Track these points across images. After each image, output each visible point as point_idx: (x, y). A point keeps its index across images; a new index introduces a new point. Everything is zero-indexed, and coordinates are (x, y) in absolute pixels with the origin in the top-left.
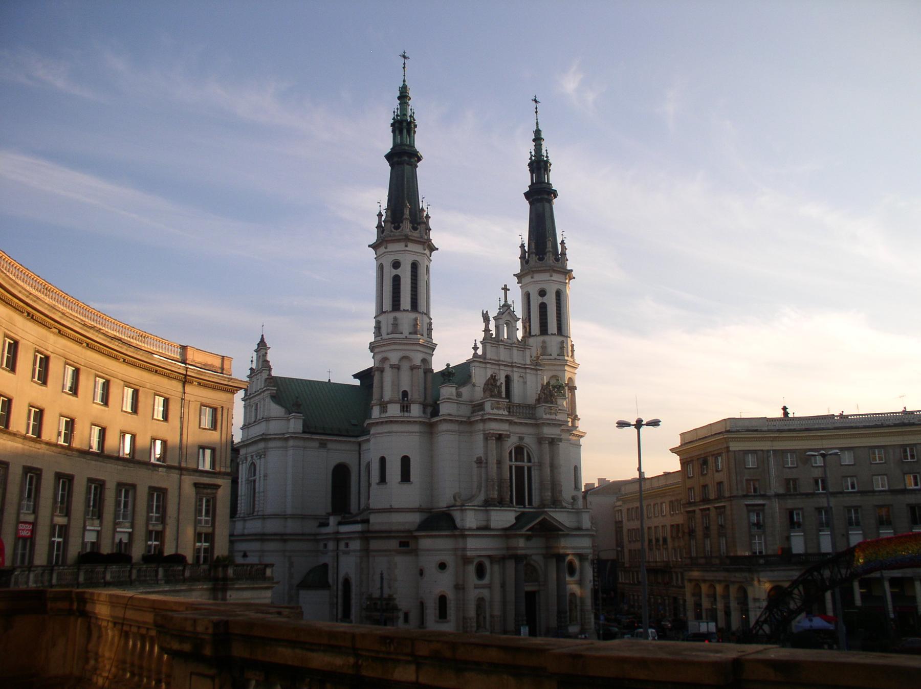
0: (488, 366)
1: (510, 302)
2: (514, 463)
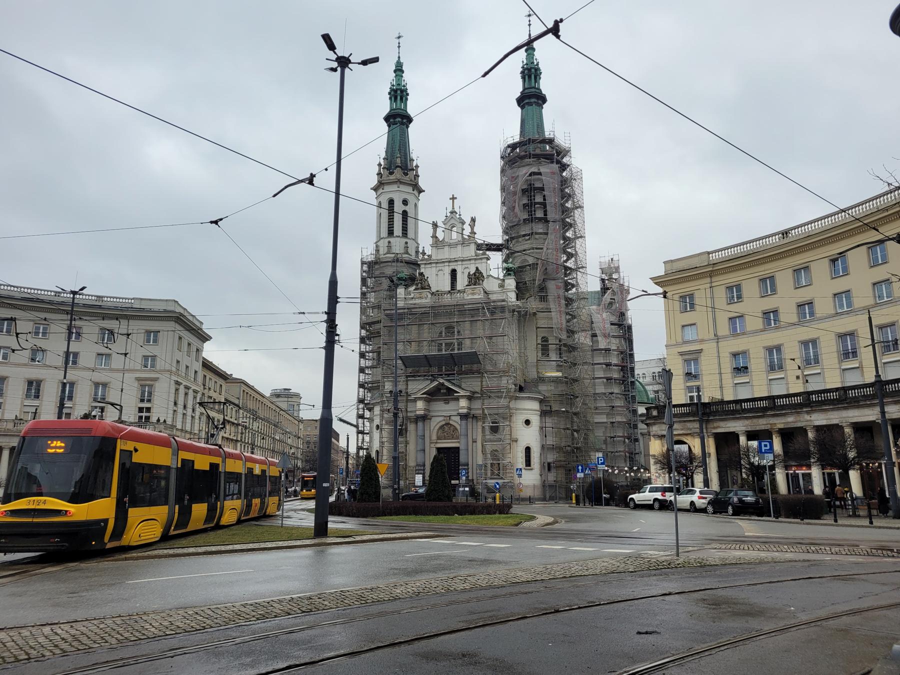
1: (457, 210)
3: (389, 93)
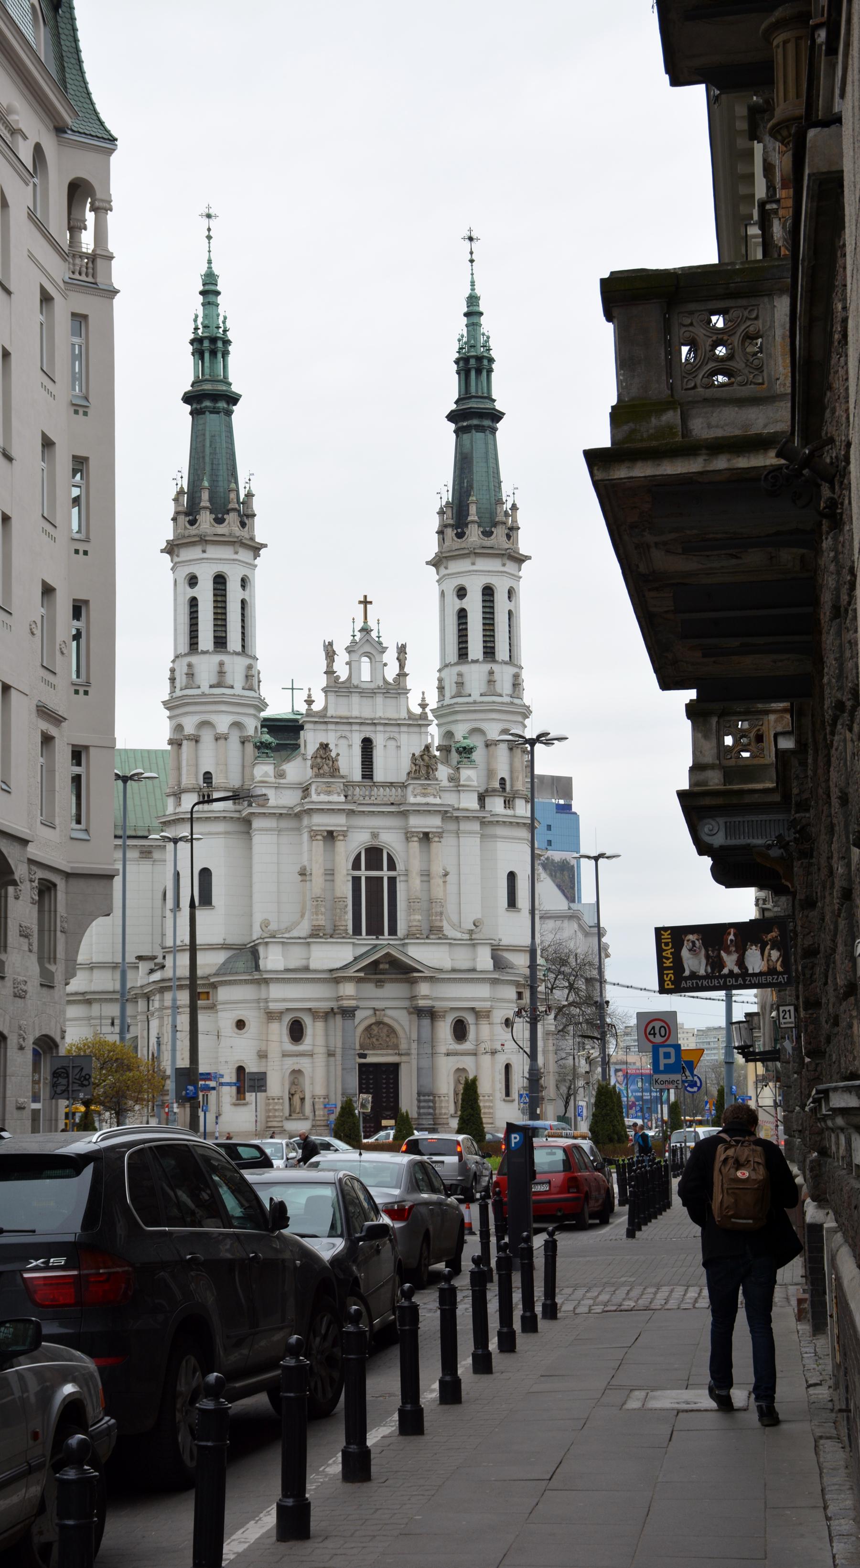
0: (331, 727)
1: (372, 623)
2: (363, 873)
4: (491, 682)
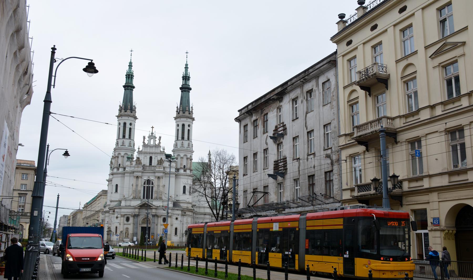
1: (153, 132)
2: (146, 185)
3: (126, 75)
4: (182, 144)
